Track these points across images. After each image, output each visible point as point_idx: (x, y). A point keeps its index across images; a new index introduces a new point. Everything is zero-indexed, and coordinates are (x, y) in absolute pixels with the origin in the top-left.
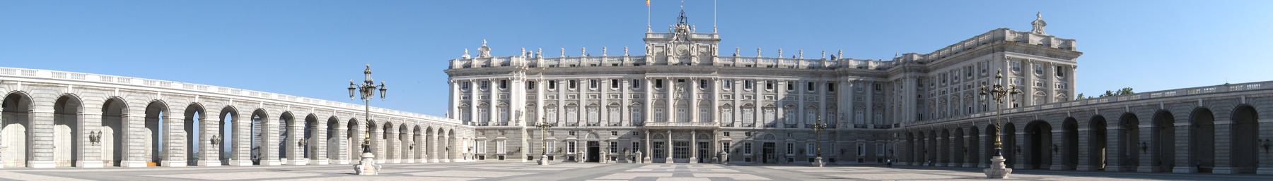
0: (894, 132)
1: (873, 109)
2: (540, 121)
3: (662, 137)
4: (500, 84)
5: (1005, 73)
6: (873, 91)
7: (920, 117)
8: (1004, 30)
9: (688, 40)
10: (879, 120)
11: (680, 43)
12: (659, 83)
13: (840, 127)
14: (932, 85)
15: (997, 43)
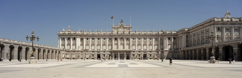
0: (179, 51)
1: (173, 45)
2: (84, 49)
3: (117, 53)
4: (73, 39)
5: (214, 31)
6: (173, 39)
7: (187, 46)
8: (214, 18)
9: (124, 28)
10: (175, 47)
11: (122, 28)
12: (116, 39)
13: (165, 50)
14: (191, 37)
15: (212, 22)
